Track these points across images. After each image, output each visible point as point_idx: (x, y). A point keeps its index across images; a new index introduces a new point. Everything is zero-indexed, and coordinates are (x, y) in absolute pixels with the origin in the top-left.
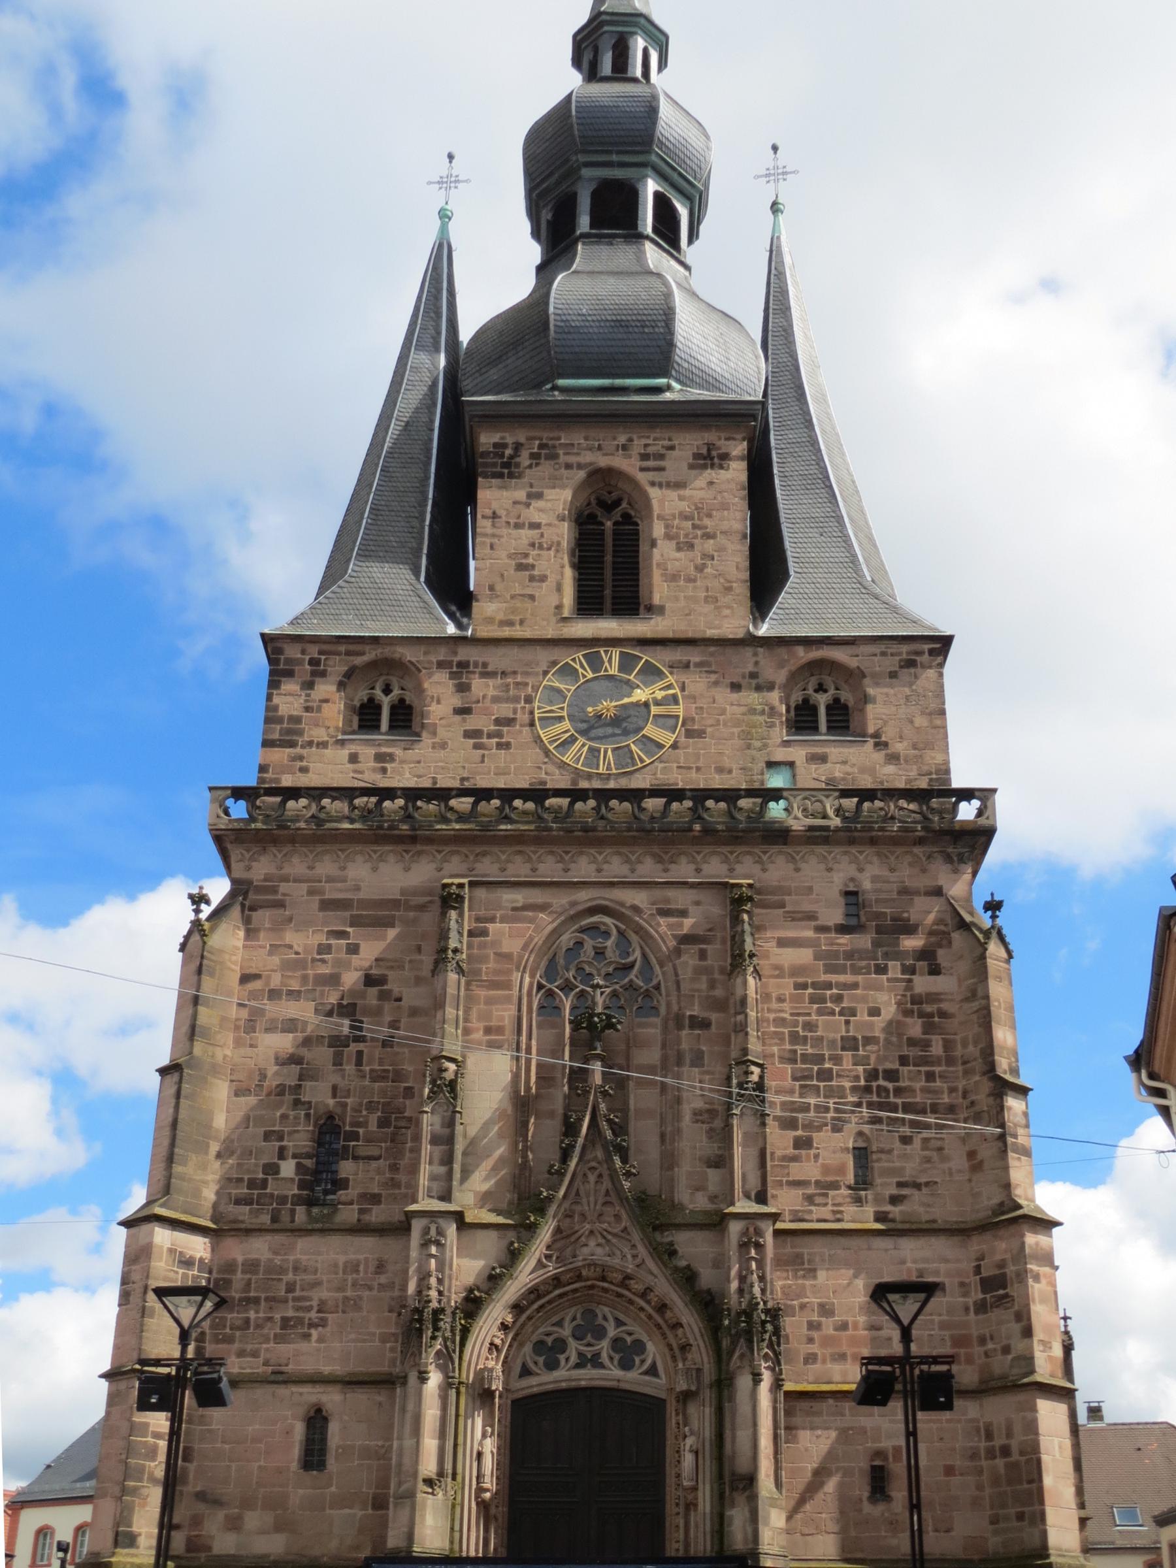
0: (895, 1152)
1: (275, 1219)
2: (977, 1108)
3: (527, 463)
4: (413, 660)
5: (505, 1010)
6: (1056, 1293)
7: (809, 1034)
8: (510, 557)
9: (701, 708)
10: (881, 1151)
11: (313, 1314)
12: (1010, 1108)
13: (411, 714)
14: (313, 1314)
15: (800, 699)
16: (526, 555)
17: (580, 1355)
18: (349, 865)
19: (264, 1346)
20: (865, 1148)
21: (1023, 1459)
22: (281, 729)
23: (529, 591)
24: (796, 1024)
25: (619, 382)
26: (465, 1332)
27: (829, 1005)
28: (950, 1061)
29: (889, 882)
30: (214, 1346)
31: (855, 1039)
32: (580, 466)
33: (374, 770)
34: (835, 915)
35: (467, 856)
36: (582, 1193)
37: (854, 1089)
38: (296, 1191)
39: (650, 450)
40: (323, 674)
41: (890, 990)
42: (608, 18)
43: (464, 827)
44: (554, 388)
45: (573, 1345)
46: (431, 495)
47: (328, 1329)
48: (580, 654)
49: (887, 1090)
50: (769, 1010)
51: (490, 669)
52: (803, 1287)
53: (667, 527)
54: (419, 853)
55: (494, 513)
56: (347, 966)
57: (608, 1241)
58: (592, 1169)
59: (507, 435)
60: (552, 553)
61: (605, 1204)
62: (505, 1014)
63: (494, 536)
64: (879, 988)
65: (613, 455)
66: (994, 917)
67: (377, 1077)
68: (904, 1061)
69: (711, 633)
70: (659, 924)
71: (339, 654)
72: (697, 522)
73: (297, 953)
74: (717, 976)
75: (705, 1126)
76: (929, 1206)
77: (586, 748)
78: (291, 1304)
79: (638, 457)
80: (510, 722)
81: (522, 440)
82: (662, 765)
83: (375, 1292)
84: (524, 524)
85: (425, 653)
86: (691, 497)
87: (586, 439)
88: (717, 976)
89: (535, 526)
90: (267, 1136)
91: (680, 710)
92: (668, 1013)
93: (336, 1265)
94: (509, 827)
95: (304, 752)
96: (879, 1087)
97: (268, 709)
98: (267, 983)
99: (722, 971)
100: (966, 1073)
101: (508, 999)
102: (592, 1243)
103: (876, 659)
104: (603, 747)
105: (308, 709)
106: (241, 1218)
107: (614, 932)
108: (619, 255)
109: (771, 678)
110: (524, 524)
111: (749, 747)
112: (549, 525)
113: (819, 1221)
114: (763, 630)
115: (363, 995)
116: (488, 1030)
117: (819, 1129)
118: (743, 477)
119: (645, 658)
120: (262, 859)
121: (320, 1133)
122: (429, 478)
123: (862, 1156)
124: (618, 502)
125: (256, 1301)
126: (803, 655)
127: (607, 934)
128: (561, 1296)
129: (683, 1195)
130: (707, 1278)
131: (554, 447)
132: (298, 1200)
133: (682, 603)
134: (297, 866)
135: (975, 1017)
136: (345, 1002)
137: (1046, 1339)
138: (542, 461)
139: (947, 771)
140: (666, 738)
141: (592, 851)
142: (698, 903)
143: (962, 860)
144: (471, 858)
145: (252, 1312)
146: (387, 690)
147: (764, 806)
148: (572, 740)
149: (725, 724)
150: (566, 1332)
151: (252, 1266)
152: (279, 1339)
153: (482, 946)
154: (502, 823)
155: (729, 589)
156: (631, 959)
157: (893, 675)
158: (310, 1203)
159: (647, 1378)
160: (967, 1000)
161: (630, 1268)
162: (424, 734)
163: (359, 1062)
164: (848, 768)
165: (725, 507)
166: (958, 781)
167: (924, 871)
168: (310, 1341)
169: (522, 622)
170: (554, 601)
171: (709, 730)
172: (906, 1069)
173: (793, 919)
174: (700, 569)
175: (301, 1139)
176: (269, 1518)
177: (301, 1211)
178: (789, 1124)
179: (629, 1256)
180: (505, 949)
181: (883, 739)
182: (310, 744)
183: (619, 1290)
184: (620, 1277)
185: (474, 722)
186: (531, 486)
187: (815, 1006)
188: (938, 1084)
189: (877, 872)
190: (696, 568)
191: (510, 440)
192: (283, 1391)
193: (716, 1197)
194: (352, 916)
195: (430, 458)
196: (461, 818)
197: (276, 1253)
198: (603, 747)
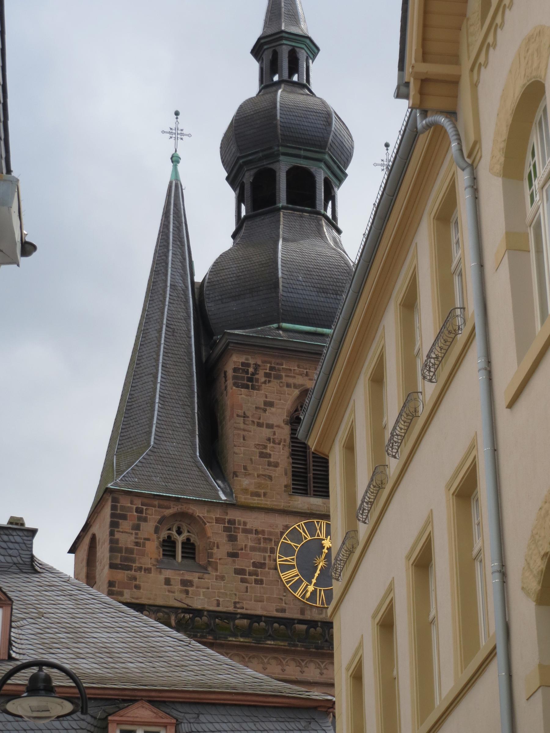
3: (263, 379)
4: (201, 515)
13: (194, 549)
16: (265, 447)
23: (267, 473)
25: (320, 330)
32: (296, 387)
33: (181, 591)
35: (243, 658)
40: (145, 520)
42: (286, 35)
43: (246, 640)
44: (279, 328)
46: (196, 390)
51: (248, 527)
59: (249, 357)
60: (281, 446)
63: (244, 430)
71: (154, 506)
80: (262, 565)
81: (259, 363)
85: (208, 512)
94: (272, 643)
95: (137, 574)
105: (137, 544)
112: (278, 426)
122: (193, 376)
138: (272, 379)
141: (317, 661)
144: (247, 659)
146: (179, 532)
154: (269, 640)
169: (265, 494)
182: (140, 569)
185: (240, 563)
186: (266, 397)
191: (252, 361)
195: (192, 360)
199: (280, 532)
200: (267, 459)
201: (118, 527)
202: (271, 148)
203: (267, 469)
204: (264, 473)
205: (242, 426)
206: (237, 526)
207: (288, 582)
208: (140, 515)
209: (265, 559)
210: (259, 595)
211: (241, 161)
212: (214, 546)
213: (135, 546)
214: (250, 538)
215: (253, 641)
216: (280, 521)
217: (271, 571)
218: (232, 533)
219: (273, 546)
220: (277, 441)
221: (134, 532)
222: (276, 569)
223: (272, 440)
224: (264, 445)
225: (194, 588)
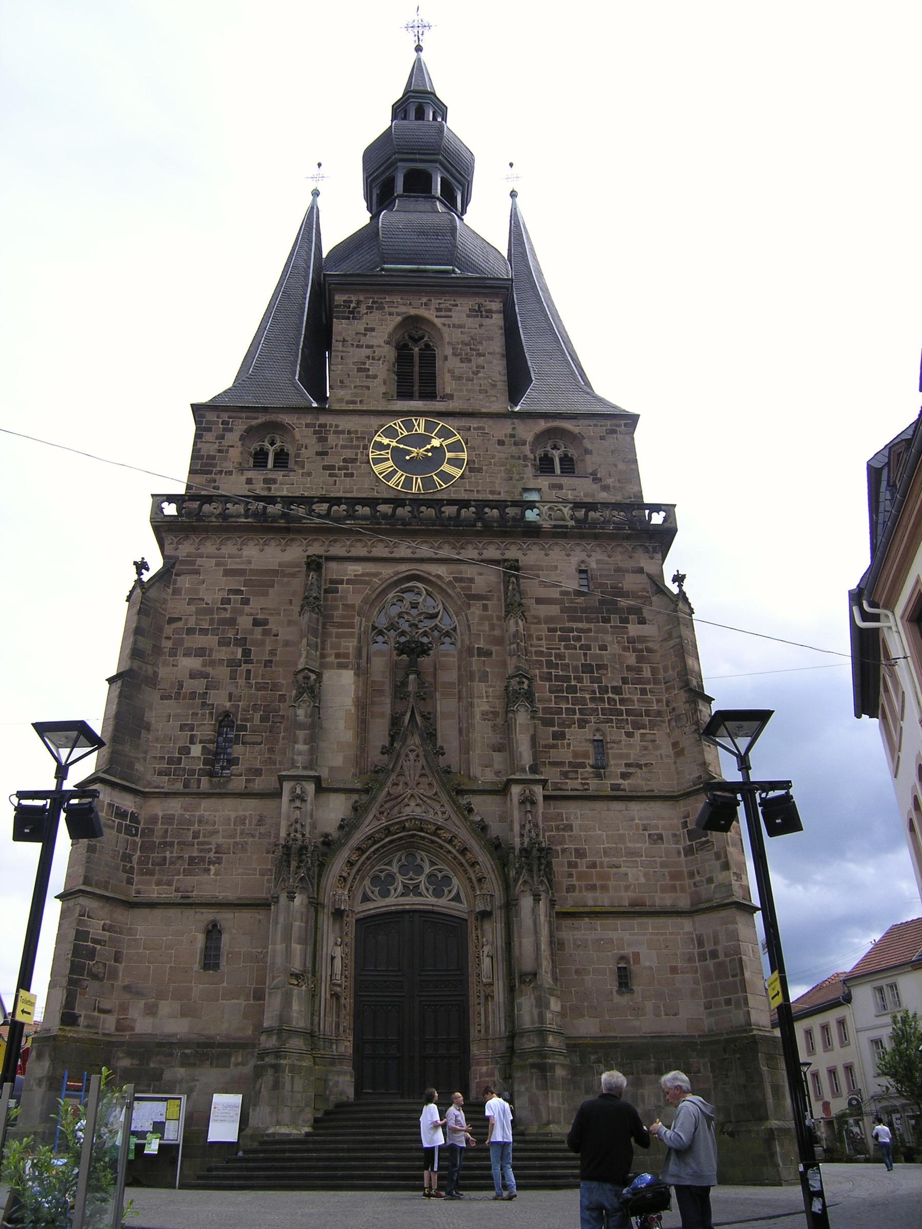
0: (623, 742)
1: (186, 786)
2: (677, 712)
3: (365, 311)
4: (290, 422)
5: (348, 642)
6: (741, 839)
7: (560, 662)
8: (354, 363)
9: (479, 455)
10: (614, 742)
11: (212, 855)
12: (701, 711)
14: (212, 855)
16: (364, 364)
17: (405, 886)
18: (244, 547)
19: (177, 877)
20: (601, 741)
21: (728, 959)
23: (365, 384)
24: (550, 655)
26: (322, 866)
27: (572, 642)
28: (656, 682)
29: (608, 564)
30: (139, 877)
31: (591, 665)
32: (398, 314)
33: (262, 489)
34: (572, 584)
36: (405, 768)
37: (593, 700)
38: (202, 766)
39: (442, 306)
40: (231, 430)
41: (612, 633)
44: (383, 269)
45: (400, 878)
46: (303, 333)
47: (223, 865)
48: (399, 421)
49: (614, 700)
50: (532, 646)
51: (340, 429)
52: (564, 836)
53: (453, 349)
54: (292, 540)
56: (241, 612)
57: (425, 802)
58: (412, 751)
60: (381, 362)
61: (422, 775)
62: (350, 645)
63: (342, 352)
64: (605, 632)
66: (680, 586)
67: (260, 687)
68: (625, 681)
69: (484, 410)
72: (472, 346)
73: (206, 604)
74: (495, 621)
75: (490, 722)
76: (649, 780)
77: (403, 477)
78: (196, 846)
80: (354, 461)
81: (362, 298)
83: (256, 839)
84: (363, 346)
86: (469, 333)
87: (402, 299)
88: (495, 621)
89: (371, 347)
90: (182, 727)
91: (464, 456)
92: (462, 646)
93: (229, 819)
94: (353, 522)
96: (608, 697)
98: (186, 624)
99: (499, 618)
100: (667, 689)
101: (352, 635)
102: (413, 804)
104: (415, 477)
105: (220, 451)
106: (162, 785)
107: (425, 592)
108: (423, 205)
109: (524, 438)
110: (363, 346)
111: (511, 479)
112: (379, 346)
113: (571, 790)
114: (517, 409)
115: (251, 632)
116: (338, 656)
117: (569, 726)
118: (501, 323)
119: (442, 423)
120: (185, 542)
121: (220, 727)
123: (600, 745)
124: (422, 338)
125: (171, 844)
126: (543, 425)
128: (391, 842)
129: (476, 770)
130: (495, 829)
131: (382, 303)
132: (203, 773)
133: (465, 393)
134: (209, 548)
135: (672, 651)
137: (738, 872)
139: (642, 497)
140: (457, 473)
142: (481, 574)
143: (655, 551)
145: (168, 853)
146: (272, 444)
147: (523, 515)
148: (394, 472)
150: (395, 869)
151: (168, 819)
152: (187, 872)
153: (335, 599)
154: (348, 520)
155: (494, 386)
156: (436, 610)
157: (602, 438)
158: (211, 774)
159: (453, 903)
160: (665, 640)
161: (440, 821)
163: (248, 677)
164: (575, 493)
165: (490, 339)
166: (647, 500)
167: (631, 557)
168: (209, 874)
169: (361, 402)
170: (383, 389)
171: (484, 468)
172: (627, 686)
173: (545, 586)
174: (476, 373)
175: (206, 729)
176: (177, 1006)
177: (205, 780)
178: (548, 723)
179: (439, 813)
181: (598, 476)
182: (221, 472)
183: (433, 838)
184: (433, 828)
186: (367, 324)
187: (563, 643)
188: (649, 696)
189: (599, 557)
190: (473, 373)
192: (189, 913)
193: (499, 772)
196: (320, 516)
197: (186, 810)
198: (415, 477)
201: (201, 438)
202: (389, 158)
206: (328, 428)
207: (380, 474)
209: (356, 455)
216: (374, 421)
217: (363, 465)
220: (376, 358)
222: (369, 462)
225: (277, 485)
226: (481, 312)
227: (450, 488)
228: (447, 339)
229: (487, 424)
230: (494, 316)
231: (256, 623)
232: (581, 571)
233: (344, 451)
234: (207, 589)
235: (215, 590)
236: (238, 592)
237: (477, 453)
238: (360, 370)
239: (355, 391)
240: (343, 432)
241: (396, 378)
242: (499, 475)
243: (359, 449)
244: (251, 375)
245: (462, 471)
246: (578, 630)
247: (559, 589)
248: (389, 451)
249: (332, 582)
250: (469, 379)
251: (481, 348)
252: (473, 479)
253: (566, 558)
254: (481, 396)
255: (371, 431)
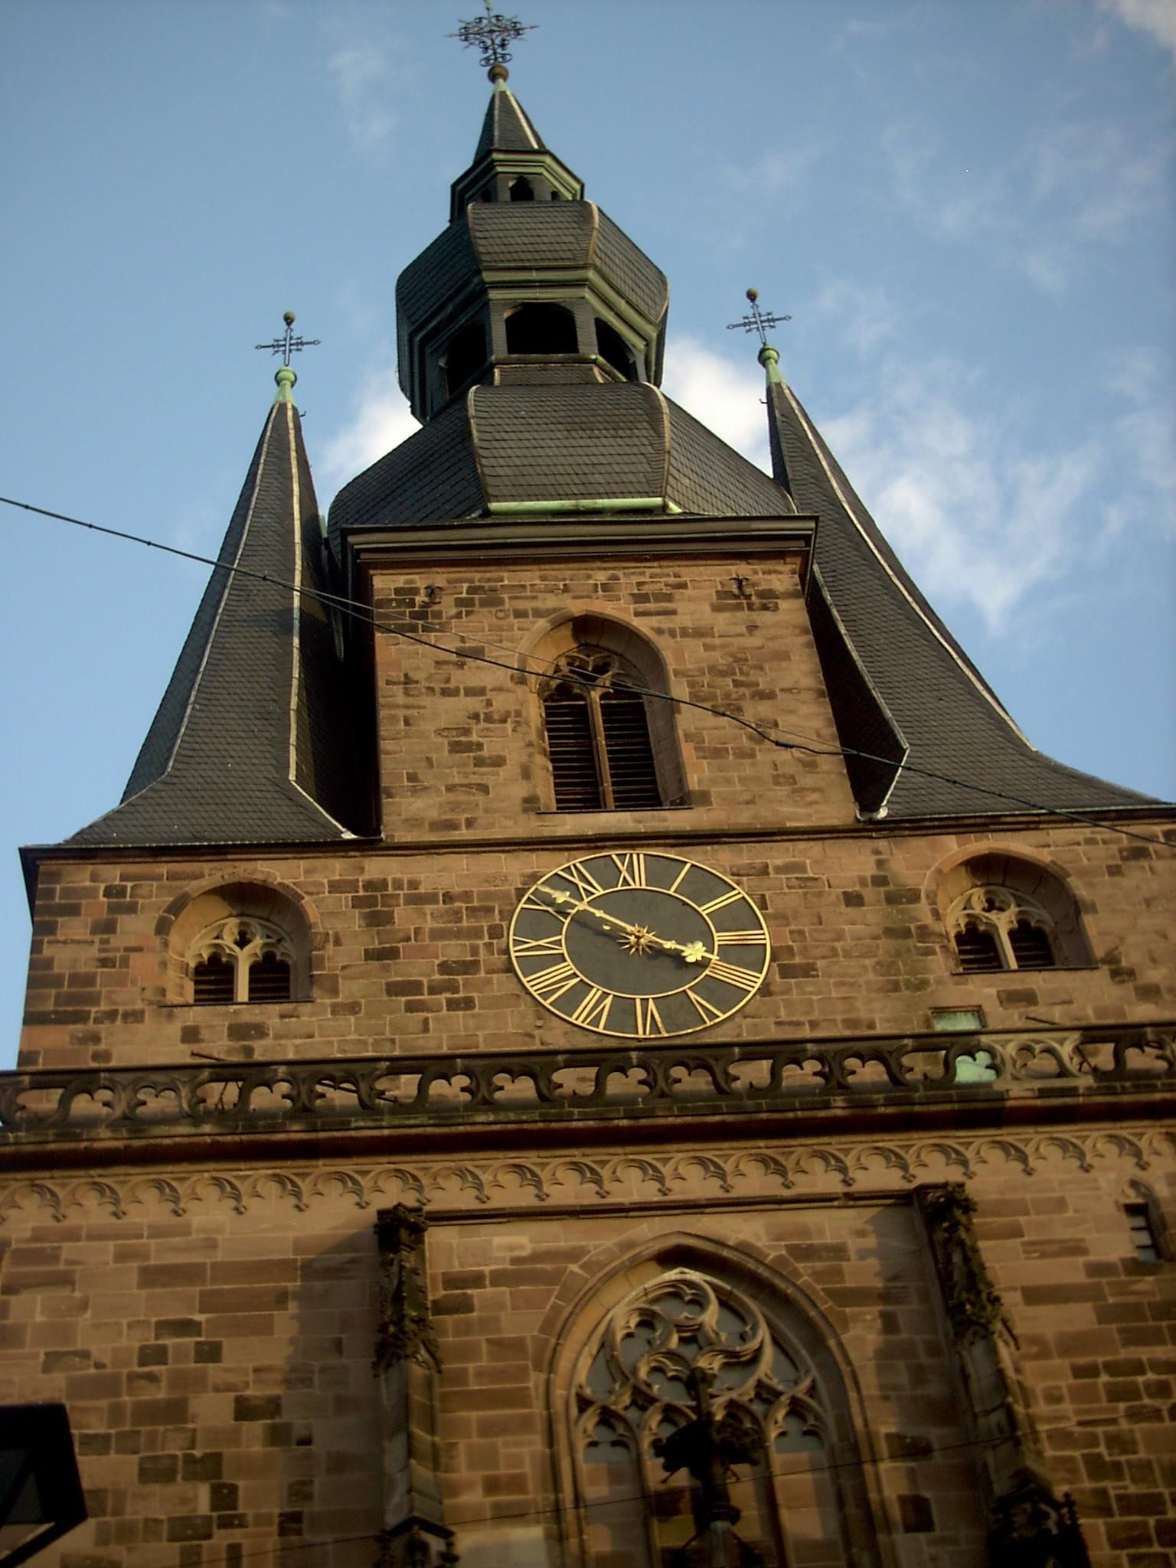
3: (454, 611)
7: (1123, 1458)
8: (439, 732)
9: (801, 933)
15: (963, 922)
16: (467, 732)
22: (58, 996)
24: (1093, 1441)
27: (1147, 1401)
32: (538, 613)
39: (646, 589)
40: (132, 909)
46: (296, 674)
51: (422, 890)
53: (691, 685)
55: (406, 676)
56: (199, 1382)
60: (509, 726)
63: (407, 707)
65: (589, 597)
70: (799, 1275)
72: (739, 677)
73: (99, 1366)
74: (924, 1359)
77: (608, 1001)
79: (630, 598)
80: (470, 967)
82: (749, 1020)
86: (723, 646)
87: (543, 578)
88: (924, 1359)
89: (479, 692)
91: (764, 936)
95: (103, 1028)
97: (33, 965)
101: (526, 1424)
103: (1080, 849)
105: (105, 962)
111: (895, 987)
112: (499, 689)
115: (234, 1438)
116: (492, 1486)
118: (804, 619)
127: (699, 1302)
131: (494, 590)
133: (738, 787)
136: (197, 1453)
138: (477, 608)
149: (847, 954)
156: (753, 1345)
162: (316, 992)
164: (1074, 1008)
165: (783, 656)
170: (521, 790)
171: (820, 964)
173: (1043, 1255)
180: (508, 1333)
181: (1124, 963)
182: (112, 1015)
185: (405, 970)
186: (463, 640)
194: (203, 1294)
198: (638, 998)
199: (517, 889)
200: (471, 754)
202: (467, 283)
203: (474, 773)
204: (466, 781)
205: (401, 699)
206: (390, 891)
208: (115, 900)
209: (475, 951)
210: (462, 1033)
211: (418, 339)
212: (327, 941)
213: (97, 967)
214: (428, 912)
215: (431, 1122)
217: (495, 976)
218: (379, 908)
219: (498, 922)
220: (496, 717)
221: (97, 938)
222: (510, 969)
223: (482, 716)
224: (463, 728)
225: (268, 1042)
226: (748, 597)
227: (738, 1020)
228: (671, 666)
229: (807, 853)
230: (784, 605)
231: (244, 1410)
232: (1132, 1210)
233: (440, 943)
234: (96, 1326)
235: (118, 1324)
236: (185, 1327)
237: (793, 927)
238: (456, 748)
239: (452, 797)
240: (431, 898)
241: (550, 766)
242: (862, 980)
243: (481, 937)
244: (169, 775)
245: (762, 976)
246: (1156, 1366)
247: (1081, 1260)
248: (562, 937)
249: (452, 1281)
250: (745, 755)
251: (761, 681)
252: (795, 995)
253: (1082, 1174)
254: (783, 791)
255: (508, 893)
